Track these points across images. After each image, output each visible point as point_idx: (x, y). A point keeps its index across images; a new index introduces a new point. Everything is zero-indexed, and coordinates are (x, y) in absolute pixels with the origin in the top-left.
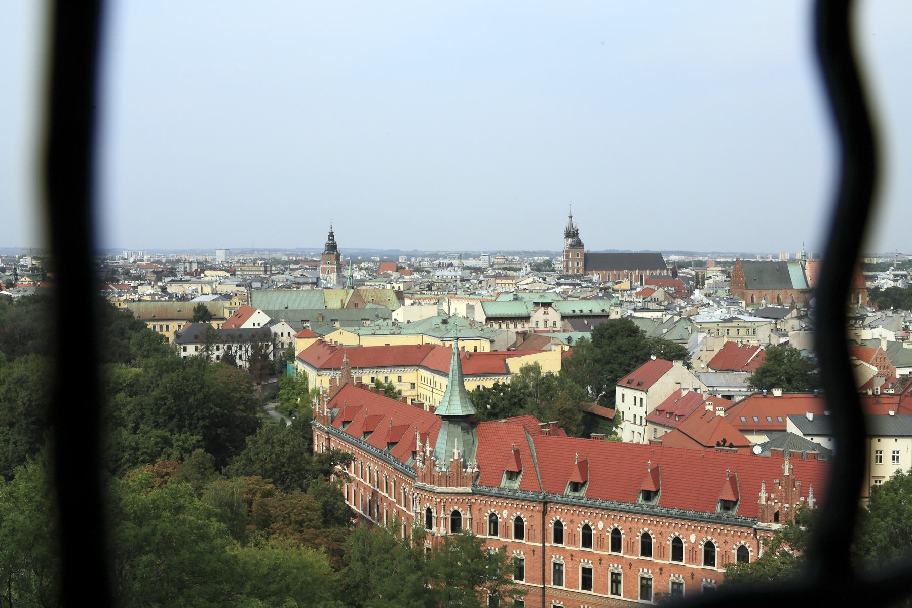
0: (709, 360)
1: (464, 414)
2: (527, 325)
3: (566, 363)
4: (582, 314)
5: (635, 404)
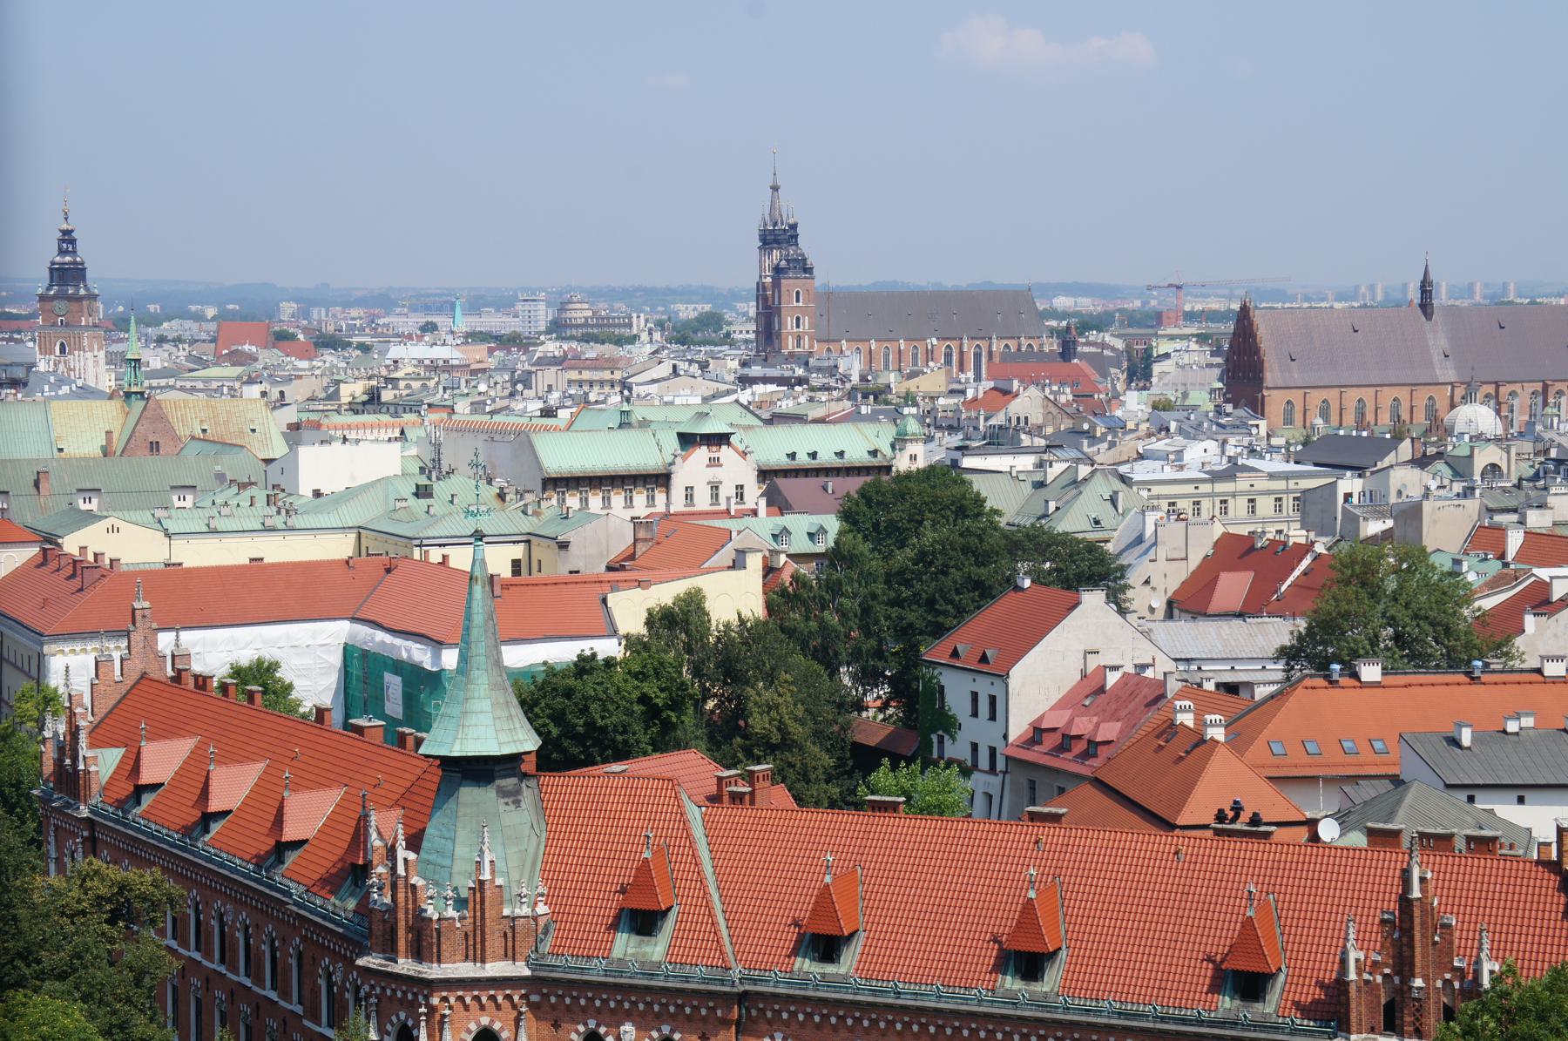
0: (1174, 584)
1: (506, 750)
2: (660, 497)
3: (780, 597)
4: (814, 464)
5: (975, 714)
